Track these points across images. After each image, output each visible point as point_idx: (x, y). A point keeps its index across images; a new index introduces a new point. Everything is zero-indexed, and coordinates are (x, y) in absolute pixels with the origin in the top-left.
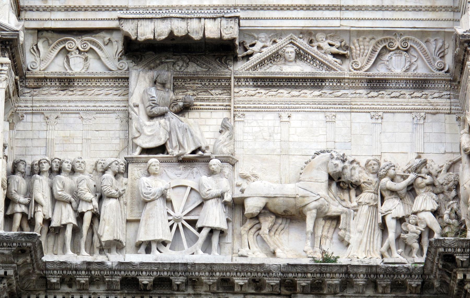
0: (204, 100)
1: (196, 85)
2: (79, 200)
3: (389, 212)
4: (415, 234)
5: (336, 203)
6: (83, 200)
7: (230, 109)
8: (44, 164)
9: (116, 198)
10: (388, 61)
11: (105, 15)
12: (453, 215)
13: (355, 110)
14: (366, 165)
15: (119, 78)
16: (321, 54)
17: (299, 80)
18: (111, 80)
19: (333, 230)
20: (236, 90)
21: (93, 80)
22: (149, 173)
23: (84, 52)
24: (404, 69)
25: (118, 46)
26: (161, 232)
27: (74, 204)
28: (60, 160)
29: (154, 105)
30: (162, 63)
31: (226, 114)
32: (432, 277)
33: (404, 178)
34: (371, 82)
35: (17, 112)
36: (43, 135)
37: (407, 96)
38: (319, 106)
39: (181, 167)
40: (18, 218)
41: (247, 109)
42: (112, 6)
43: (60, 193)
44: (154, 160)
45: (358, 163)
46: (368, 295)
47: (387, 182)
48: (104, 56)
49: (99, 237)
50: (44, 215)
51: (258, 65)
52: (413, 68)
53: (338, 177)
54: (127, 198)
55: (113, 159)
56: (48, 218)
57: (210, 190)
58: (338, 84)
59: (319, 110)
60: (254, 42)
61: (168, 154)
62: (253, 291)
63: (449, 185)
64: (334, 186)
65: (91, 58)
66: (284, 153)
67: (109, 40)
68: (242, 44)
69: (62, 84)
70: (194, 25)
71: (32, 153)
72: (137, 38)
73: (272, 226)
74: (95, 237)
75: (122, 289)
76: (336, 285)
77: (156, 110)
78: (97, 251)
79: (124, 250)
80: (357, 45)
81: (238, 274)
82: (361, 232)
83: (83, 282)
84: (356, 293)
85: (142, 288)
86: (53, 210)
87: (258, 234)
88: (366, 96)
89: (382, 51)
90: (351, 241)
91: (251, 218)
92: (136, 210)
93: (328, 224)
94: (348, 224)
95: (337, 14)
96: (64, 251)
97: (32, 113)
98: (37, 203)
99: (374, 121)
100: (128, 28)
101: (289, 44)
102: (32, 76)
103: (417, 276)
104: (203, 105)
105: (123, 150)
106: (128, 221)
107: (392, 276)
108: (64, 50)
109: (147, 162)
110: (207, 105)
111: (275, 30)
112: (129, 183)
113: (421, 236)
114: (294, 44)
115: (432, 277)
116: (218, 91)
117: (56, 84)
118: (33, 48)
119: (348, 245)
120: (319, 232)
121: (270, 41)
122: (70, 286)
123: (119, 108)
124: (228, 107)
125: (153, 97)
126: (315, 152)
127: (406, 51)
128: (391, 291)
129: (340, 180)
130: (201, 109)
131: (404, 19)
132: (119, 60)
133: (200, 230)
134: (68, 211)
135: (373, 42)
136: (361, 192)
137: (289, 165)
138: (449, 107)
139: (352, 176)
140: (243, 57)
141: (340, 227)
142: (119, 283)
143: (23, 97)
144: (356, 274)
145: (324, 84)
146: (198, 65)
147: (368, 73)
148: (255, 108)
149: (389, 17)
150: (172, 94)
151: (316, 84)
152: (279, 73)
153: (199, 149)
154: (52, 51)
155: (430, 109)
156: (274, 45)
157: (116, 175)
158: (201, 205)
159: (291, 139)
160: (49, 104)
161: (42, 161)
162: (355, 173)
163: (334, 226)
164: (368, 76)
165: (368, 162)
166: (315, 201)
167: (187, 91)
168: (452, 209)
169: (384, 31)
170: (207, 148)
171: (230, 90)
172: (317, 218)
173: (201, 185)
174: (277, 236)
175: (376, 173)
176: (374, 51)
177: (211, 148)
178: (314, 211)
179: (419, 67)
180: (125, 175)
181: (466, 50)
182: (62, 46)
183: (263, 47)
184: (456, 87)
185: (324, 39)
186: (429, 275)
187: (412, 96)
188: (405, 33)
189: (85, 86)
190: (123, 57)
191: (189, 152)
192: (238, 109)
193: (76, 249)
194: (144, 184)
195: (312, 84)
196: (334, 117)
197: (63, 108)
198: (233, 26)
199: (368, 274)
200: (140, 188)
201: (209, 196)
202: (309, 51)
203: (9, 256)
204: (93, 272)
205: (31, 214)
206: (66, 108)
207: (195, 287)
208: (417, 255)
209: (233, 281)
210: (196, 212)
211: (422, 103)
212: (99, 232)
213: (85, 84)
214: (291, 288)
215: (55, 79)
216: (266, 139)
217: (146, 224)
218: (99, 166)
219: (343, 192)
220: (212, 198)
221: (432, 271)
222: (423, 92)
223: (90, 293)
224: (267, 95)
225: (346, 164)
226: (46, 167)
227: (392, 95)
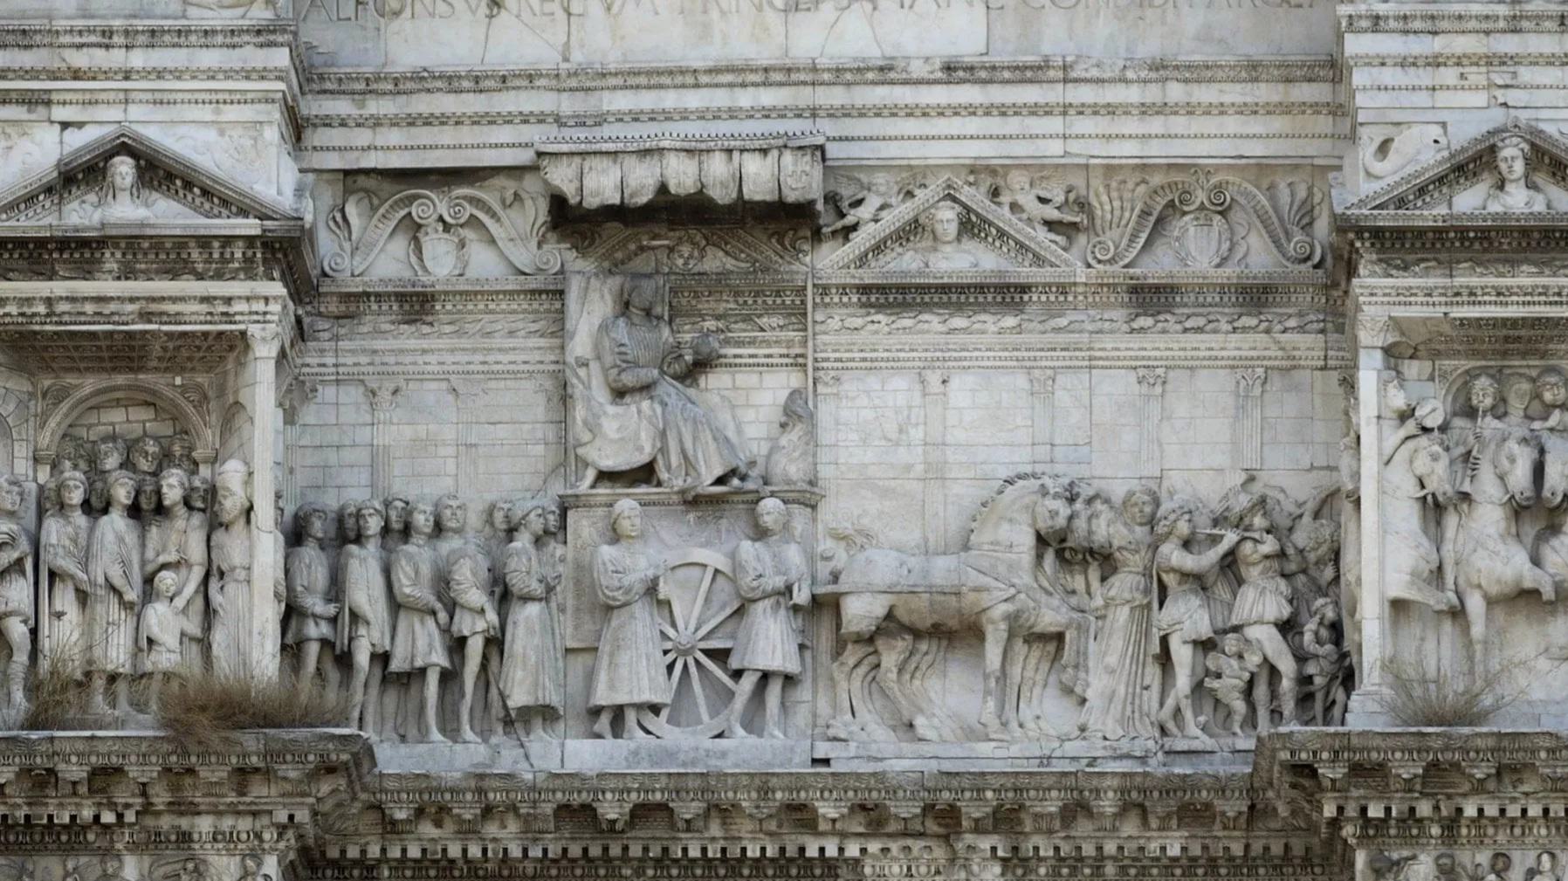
0: (743, 342)
1: (724, 305)
2: (452, 607)
3: (1177, 627)
4: (1237, 682)
5: (1055, 602)
6: (463, 607)
7: (805, 365)
8: (369, 519)
9: (540, 600)
10: (1178, 239)
11: (504, 134)
12: (1324, 633)
13: (1101, 363)
14: (1124, 503)
15: (540, 292)
16: (1020, 225)
17: (969, 288)
18: (522, 297)
19: (1048, 664)
20: (819, 317)
21: (479, 297)
22: (615, 535)
23: (457, 225)
24: (1217, 260)
25: (536, 212)
26: (645, 683)
27: (443, 616)
28: (407, 503)
29: (624, 365)
30: (642, 249)
31: (794, 379)
32: (1270, 794)
33: (1215, 540)
34: (1137, 292)
35: (301, 378)
36: (364, 435)
37: (1226, 327)
38: (1016, 353)
39: (691, 516)
40: (313, 649)
41: (845, 365)
42: (521, 113)
43: (407, 590)
44: (627, 504)
45: (1107, 501)
46: (1126, 835)
47: (1172, 554)
48: (503, 235)
49: (503, 698)
50: (373, 645)
51: (871, 255)
52: (1240, 252)
53: (1058, 539)
54: (565, 593)
55: (530, 504)
56: (381, 651)
57: (761, 576)
58: (1061, 298)
59: (1015, 363)
60: (860, 196)
61: (659, 484)
62: (861, 830)
63: (1320, 552)
64: (1050, 557)
65: (471, 241)
66: (936, 473)
67: (516, 196)
68: (832, 199)
69: (407, 307)
70: (718, 168)
71: (339, 482)
72: (581, 202)
73: (906, 661)
74: (494, 692)
75: (557, 829)
76: (1051, 815)
77: (628, 379)
78: (500, 729)
79: (561, 726)
80: (1105, 198)
81: (826, 794)
82: (1113, 672)
83: (468, 817)
84: (1099, 830)
85: (604, 826)
86: (394, 629)
87: (874, 678)
88: (1125, 327)
89: (1166, 213)
90: (1089, 694)
91: (856, 642)
92: (589, 626)
93: (1036, 653)
94: (1082, 654)
95: (1055, 124)
96: (423, 737)
97: (337, 380)
98: (355, 617)
99: (1145, 389)
100: (561, 177)
101: (943, 199)
102: (333, 289)
103: (1237, 794)
104: (740, 356)
105: (553, 471)
106: (568, 651)
107: (1180, 794)
108: (406, 222)
109: (611, 505)
110: (751, 356)
111: (910, 167)
112: (570, 557)
113: (1251, 684)
114: (955, 200)
115: (1270, 794)
116: (775, 321)
117: (391, 306)
118: (334, 218)
119: (1083, 701)
120: (1016, 671)
121: (899, 193)
122: (438, 824)
123: (541, 367)
124: (800, 360)
125: (622, 345)
126: (1004, 477)
127: (1220, 213)
128: (1179, 826)
129: (1064, 545)
130: (736, 365)
131: (1216, 136)
132: (539, 245)
133: (737, 674)
134: (429, 635)
135: (1142, 189)
136: (1115, 570)
137: (945, 503)
138: (1323, 353)
139: (1090, 532)
140: (834, 233)
141: (1063, 662)
142: (551, 818)
143: (314, 343)
144: (1098, 791)
145: (1026, 298)
146: (727, 253)
147: (1131, 271)
148: (864, 360)
149: (1180, 131)
150: (666, 332)
151: (1008, 300)
152: (920, 274)
153: (733, 472)
154: (381, 225)
155: (1276, 358)
156: (909, 204)
157: (538, 541)
158: (740, 612)
159: (949, 439)
160: (377, 359)
161: (364, 512)
162: (1099, 526)
163: (1051, 657)
164: (1131, 278)
165: (1131, 494)
166: (1006, 600)
167: (704, 320)
168: (1322, 619)
169: (1170, 166)
170: (752, 464)
171: (805, 315)
172: (1011, 635)
173: (737, 566)
174: (917, 682)
175: (1151, 522)
176: (1145, 213)
177: (761, 461)
178: (1003, 626)
179: (1253, 251)
180: (560, 537)
181: (1352, 244)
182: (403, 213)
183: (882, 208)
184: (1339, 302)
185: (1027, 186)
186: (1264, 790)
187: (1236, 325)
188: (1218, 168)
189: (459, 312)
190: (549, 235)
191: (709, 482)
192: (825, 365)
193: (450, 729)
194: (604, 564)
195: (999, 299)
196: (1050, 382)
197: (411, 368)
198: (808, 168)
199: (1123, 791)
200: (595, 575)
201: (758, 594)
202: (990, 217)
203: (301, 782)
204: (491, 796)
205: (343, 644)
206: (416, 368)
207: (729, 821)
208: (1241, 727)
209: (815, 810)
210: (729, 627)
211: (1258, 344)
212: (501, 686)
213: (460, 307)
214: (948, 820)
215: (389, 295)
216: (890, 440)
217: (610, 663)
218: (499, 517)
219: (1071, 572)
220: (765, 598)
221: (1271, 784)
222: (1261, 313)
223: (484, 839)
224: (894, 326)
225: (1079, 505)
226: (374, 525)
227: (1188, 324)
